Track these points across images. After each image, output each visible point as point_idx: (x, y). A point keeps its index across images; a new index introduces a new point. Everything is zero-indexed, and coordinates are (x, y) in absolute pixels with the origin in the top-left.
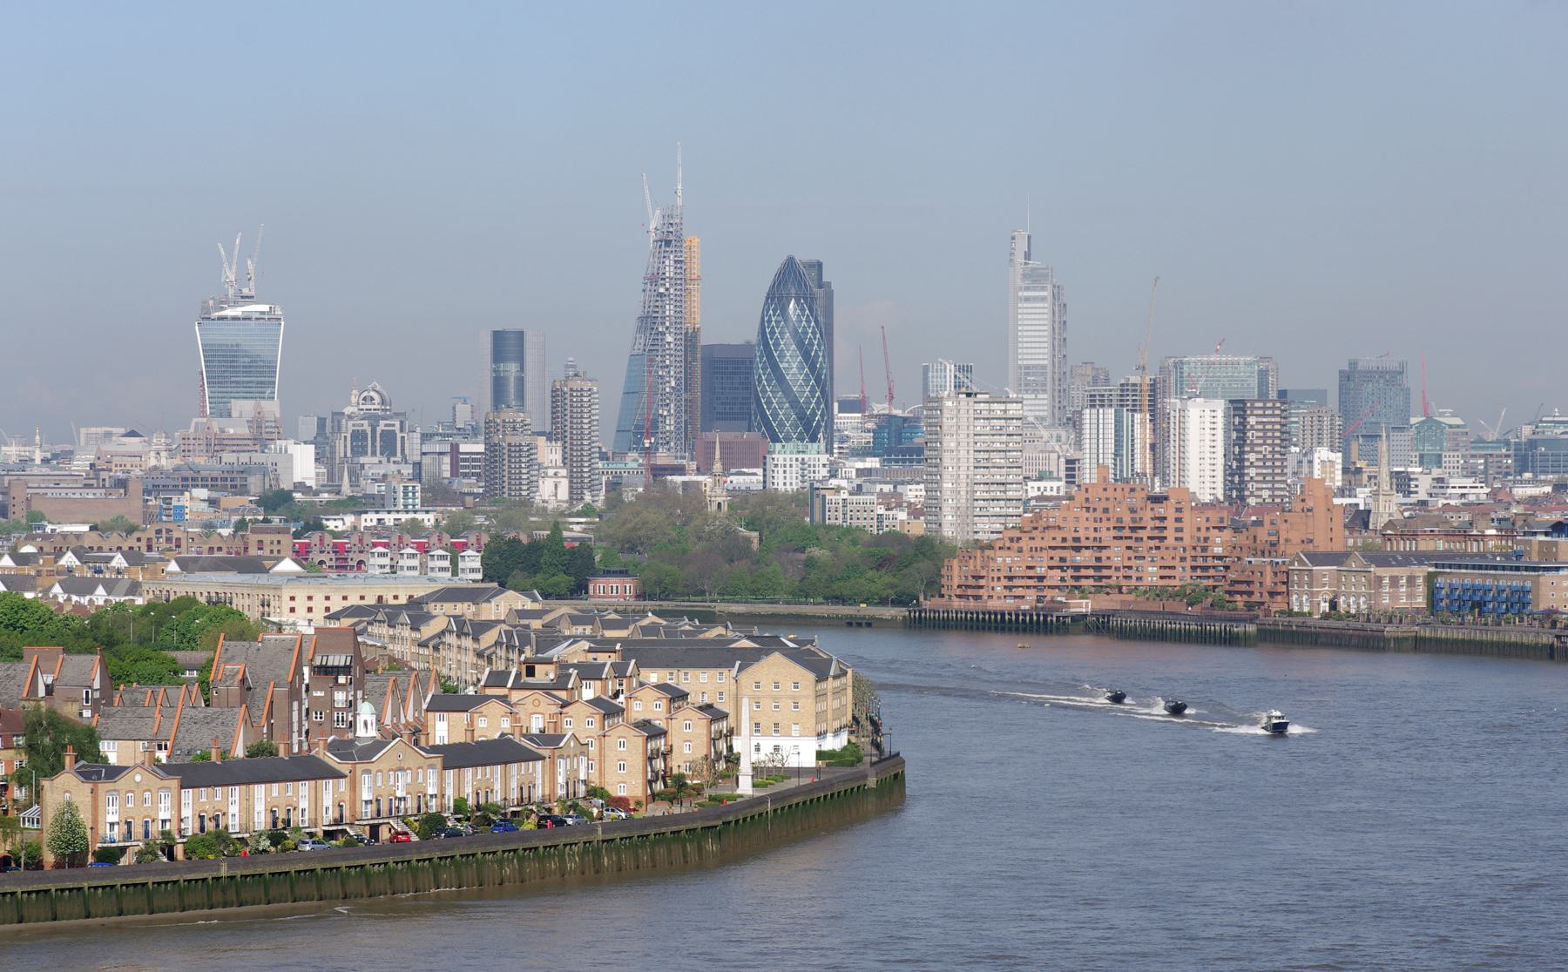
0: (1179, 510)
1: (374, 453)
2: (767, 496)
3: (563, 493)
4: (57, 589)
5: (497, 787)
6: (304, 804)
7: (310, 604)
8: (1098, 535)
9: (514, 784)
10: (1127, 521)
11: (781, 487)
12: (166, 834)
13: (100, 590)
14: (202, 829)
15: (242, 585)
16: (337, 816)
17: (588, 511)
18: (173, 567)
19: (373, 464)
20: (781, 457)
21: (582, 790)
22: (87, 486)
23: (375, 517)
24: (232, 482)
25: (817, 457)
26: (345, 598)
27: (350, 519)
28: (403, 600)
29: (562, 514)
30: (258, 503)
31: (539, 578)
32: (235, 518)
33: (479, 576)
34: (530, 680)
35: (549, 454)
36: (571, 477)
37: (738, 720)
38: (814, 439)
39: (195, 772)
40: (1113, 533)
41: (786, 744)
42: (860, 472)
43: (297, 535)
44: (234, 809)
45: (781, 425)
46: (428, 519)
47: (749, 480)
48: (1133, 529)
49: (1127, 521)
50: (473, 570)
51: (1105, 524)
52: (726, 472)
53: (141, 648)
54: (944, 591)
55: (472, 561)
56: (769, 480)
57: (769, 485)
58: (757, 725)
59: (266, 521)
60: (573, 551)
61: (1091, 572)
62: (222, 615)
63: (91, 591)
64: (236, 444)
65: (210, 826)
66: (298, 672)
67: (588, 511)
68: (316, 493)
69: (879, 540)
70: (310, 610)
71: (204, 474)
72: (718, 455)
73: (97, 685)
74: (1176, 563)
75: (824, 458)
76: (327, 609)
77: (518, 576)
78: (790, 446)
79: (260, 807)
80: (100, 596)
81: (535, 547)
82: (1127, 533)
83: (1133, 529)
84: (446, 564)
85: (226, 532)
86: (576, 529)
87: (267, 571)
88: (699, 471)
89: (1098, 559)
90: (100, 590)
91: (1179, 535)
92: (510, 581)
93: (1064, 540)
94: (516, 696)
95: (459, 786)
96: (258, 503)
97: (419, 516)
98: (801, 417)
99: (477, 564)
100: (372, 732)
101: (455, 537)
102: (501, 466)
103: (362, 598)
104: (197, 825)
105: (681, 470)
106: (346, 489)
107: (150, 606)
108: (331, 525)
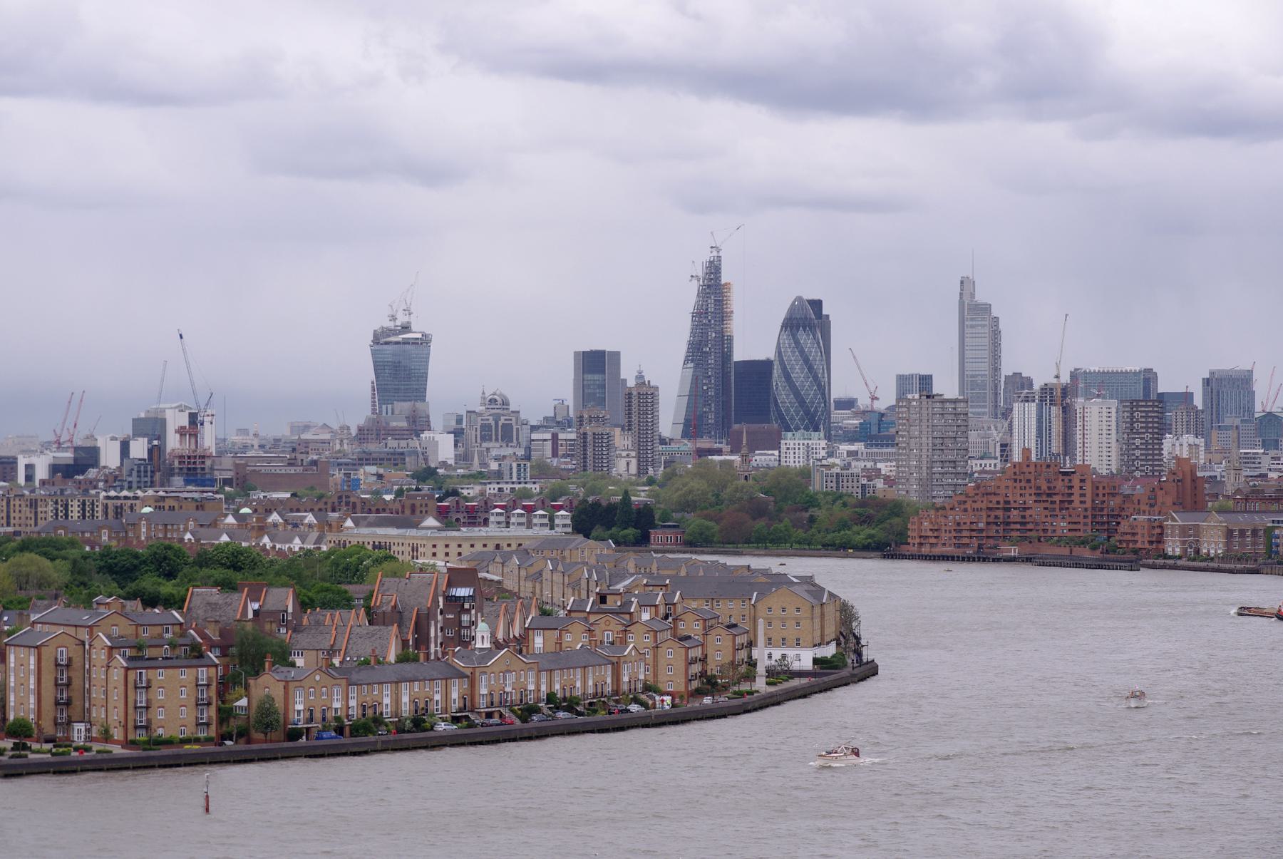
1: (497, 440)
2: (784, 472)
3: (633, 469)
4: (266, 540)
5: (578, 684)
6: (437, 697)
7: (447, 550)
9: (590, 683)
10: (1044, 487)
11: (792, 464)
12: (337, 719)
13: (297, 541)
15: (398, 536)
17: (651, 482)
18: (349, 523)
19: (497, 449)
20: (792, 442)
21: (640, 686)
22: (290, 465)
23: (497, 486)
24: (396, 459)
25: (819, 443)
26: (472, 546)
27: (478, 488)
29: (632, 484)
30: (413, 477)
31: (614, 530)
32: (396, 487)
33: (570, 530)
34: (603, 606)
35: (622, 440)
36: (638, 457)
37: (756, 636)
38: (816, 429)
39: (349, 675)
40: (1034, 498)
41: (791, 653)
42: (850, 453)
43: (440, 500)
44: (387, 701)
45: (792, 419)
46: (535, 488)
47: (764, 458)
48: (1049, 495)
49: (1044, 487)
50: (564, 526)
51: (1028, 491)
52: (752, 449)
53: (333, 583)
54: (909, 540)
55: (563, 517)
56: (783, 460)
57: (783, 464)
58: (770, 639)
59: (418, 489)
60: (639, 512)
61: (1018, 526)
62: (384, 555)
63: (290, 541)
64: (398, 434)
65: (370, 713)
66: (435, 601)
67: (651, 482)
68: (455, 469)
69: (863, 504)
70: (447, 554)
71: (374, 456)
72: (744, 442)
73: (290, 610)
74: (1081, 519)
75: (823, 443)
76: (460, 554)
77: (598, 531)
78: (798, 434)
79: (405, 699)
80: (297, 544)
81: (612, 508)
82: (1044, 498)
83: (1049, 495)
84: (546, 521)
85: (388, 497)
86: (640, 496)
87: (416, 526)
88: (732, 452)
89: (1024, 517)
90: (297, 541)
92: (594, 533)
93: (998, 503)
94: (592, 618)
95: (550, 684)
96: (413, 477)
97: (528, 486)
98: (807, 413)
99: (569, 522)
100: (487, 645)
101: (550, 502)
102: (592, 450)
103: (485, 546)
104: (360, 712)
105: (719, 452)
106: (476, 467)
107: (330, 553)
108: (465, 492)
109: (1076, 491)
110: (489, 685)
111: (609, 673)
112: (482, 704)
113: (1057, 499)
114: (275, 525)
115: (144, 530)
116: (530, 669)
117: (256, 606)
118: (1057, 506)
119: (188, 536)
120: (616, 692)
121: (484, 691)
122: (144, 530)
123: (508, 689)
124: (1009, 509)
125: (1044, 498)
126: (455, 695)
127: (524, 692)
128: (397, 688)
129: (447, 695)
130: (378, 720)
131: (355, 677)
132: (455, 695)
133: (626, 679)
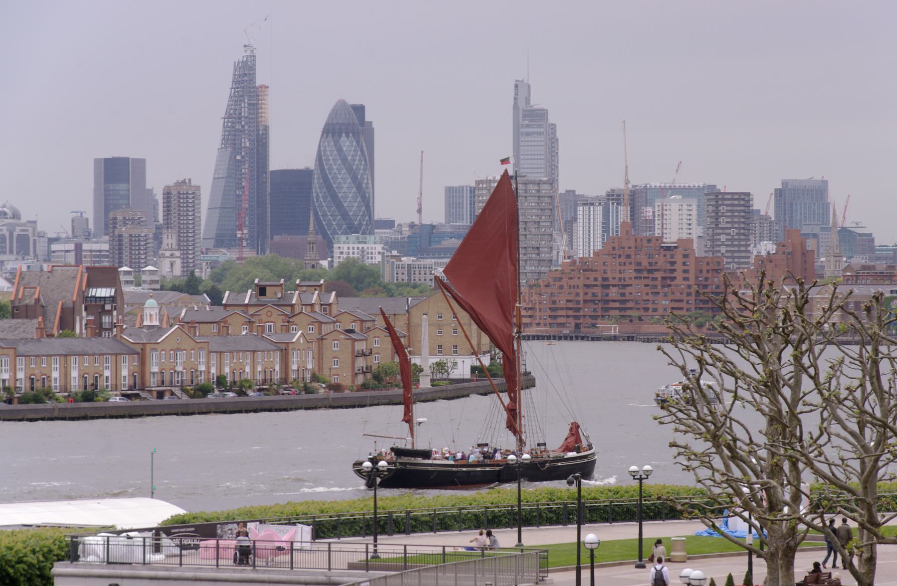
0: (686, 256)
5: (248, 369)
6: (107, 373)
8: (622, 276)
10: (645, 263)
14: (32, 389)
16: (132, 382)
21: (308, 376)
34: (263, 298)
44: (55, 374)
48: (650, 271)
49: (645, 263)
61: (617, 305)
65: (38, 385)
79: (75, 374)
82: (645, 274)
83: (650, 271)
89: (623, 294)
91: (686, 275)
93: (596, 279)
94: (252, 311)
95: (220, 367)
104: (28, 385)
109: (679, 267)
110: (159, 364)
111: (278, 360)
112: (153, 382)
113: (658, 275)
116: (201, 349)
118: (659, 283)
120: (285, 380)
121: (155, 369)
123: (179, 368)
124: (606, 287)
125: (645, 274)
126: (125, 372)
127: (194, 373)
128: (66, 362)
129: (116, 372)
130: (49, 394)
131: (21, 349)
132: (125, 372)
133: (294, 367)
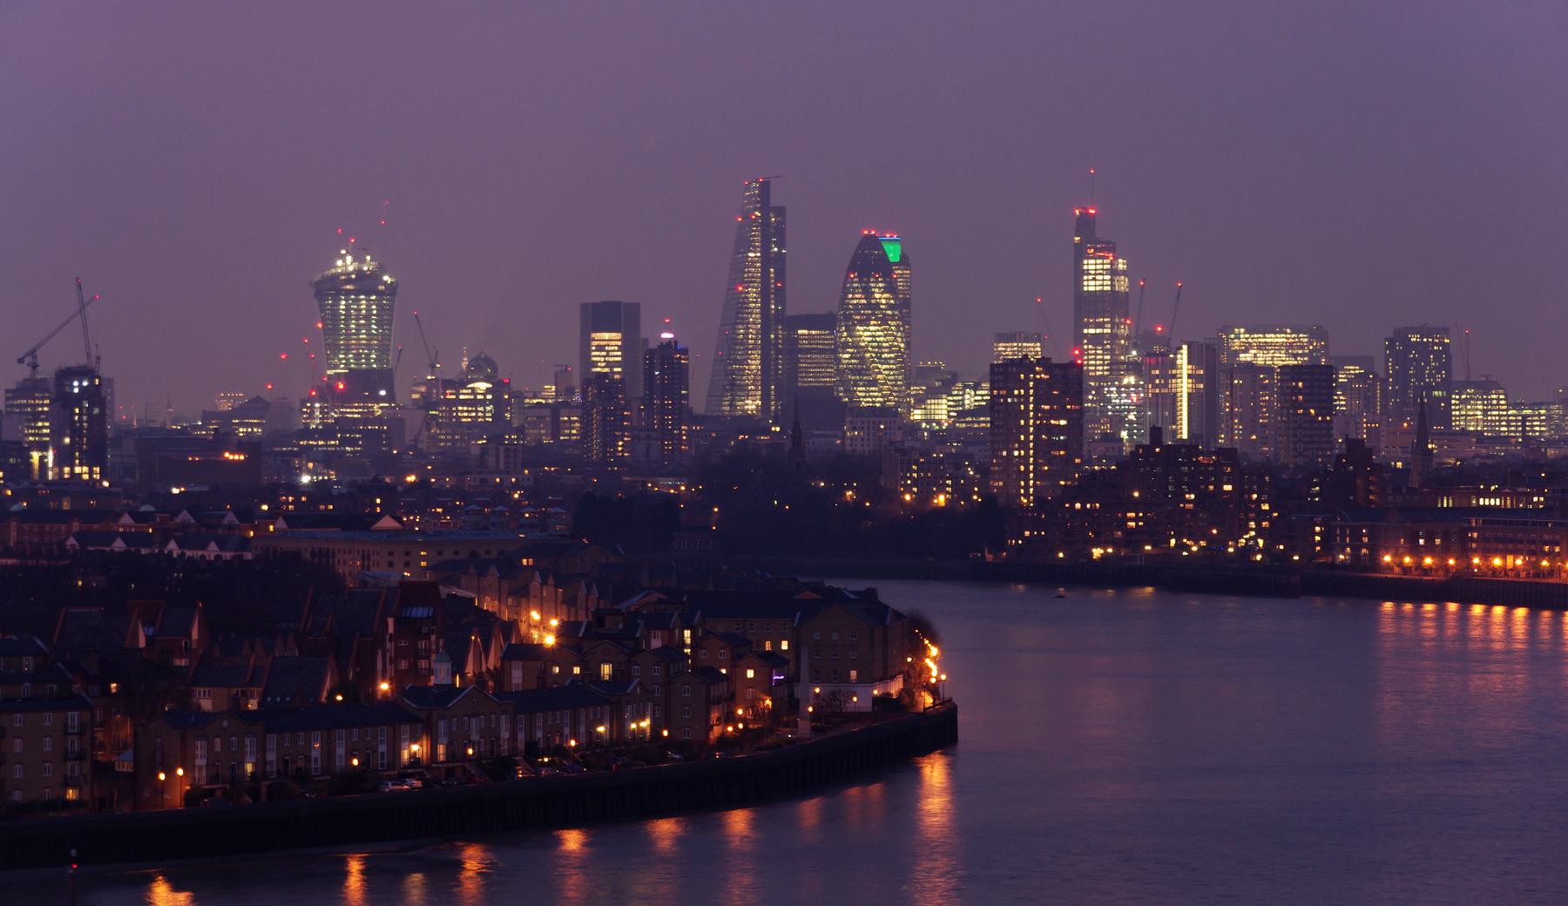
4: (172, 545)
6: (382, 748)
13: (213, 547)
26: (440, 553)
28: (494, 555)
63: (204, 546)
80: (212, 551)
90: (213, 547)
95: (530, 732)
114: (185, 526)
115: (13, 534)
117: (151, 632)
119: (71, 541)
122: (13, 534)
